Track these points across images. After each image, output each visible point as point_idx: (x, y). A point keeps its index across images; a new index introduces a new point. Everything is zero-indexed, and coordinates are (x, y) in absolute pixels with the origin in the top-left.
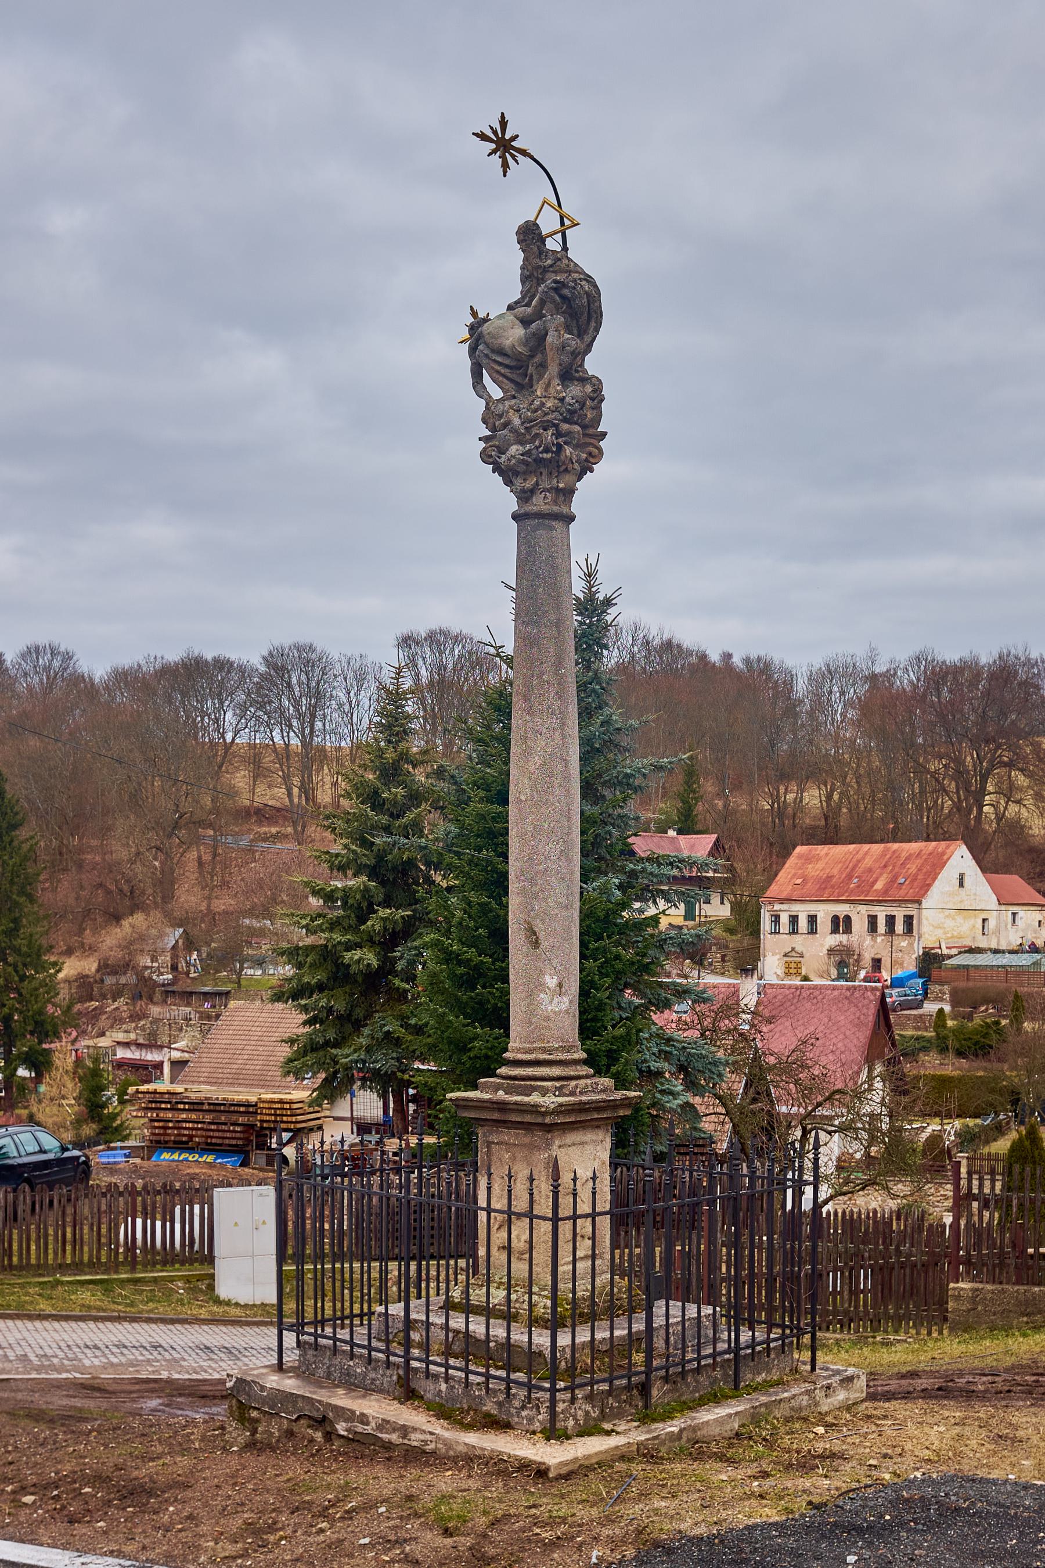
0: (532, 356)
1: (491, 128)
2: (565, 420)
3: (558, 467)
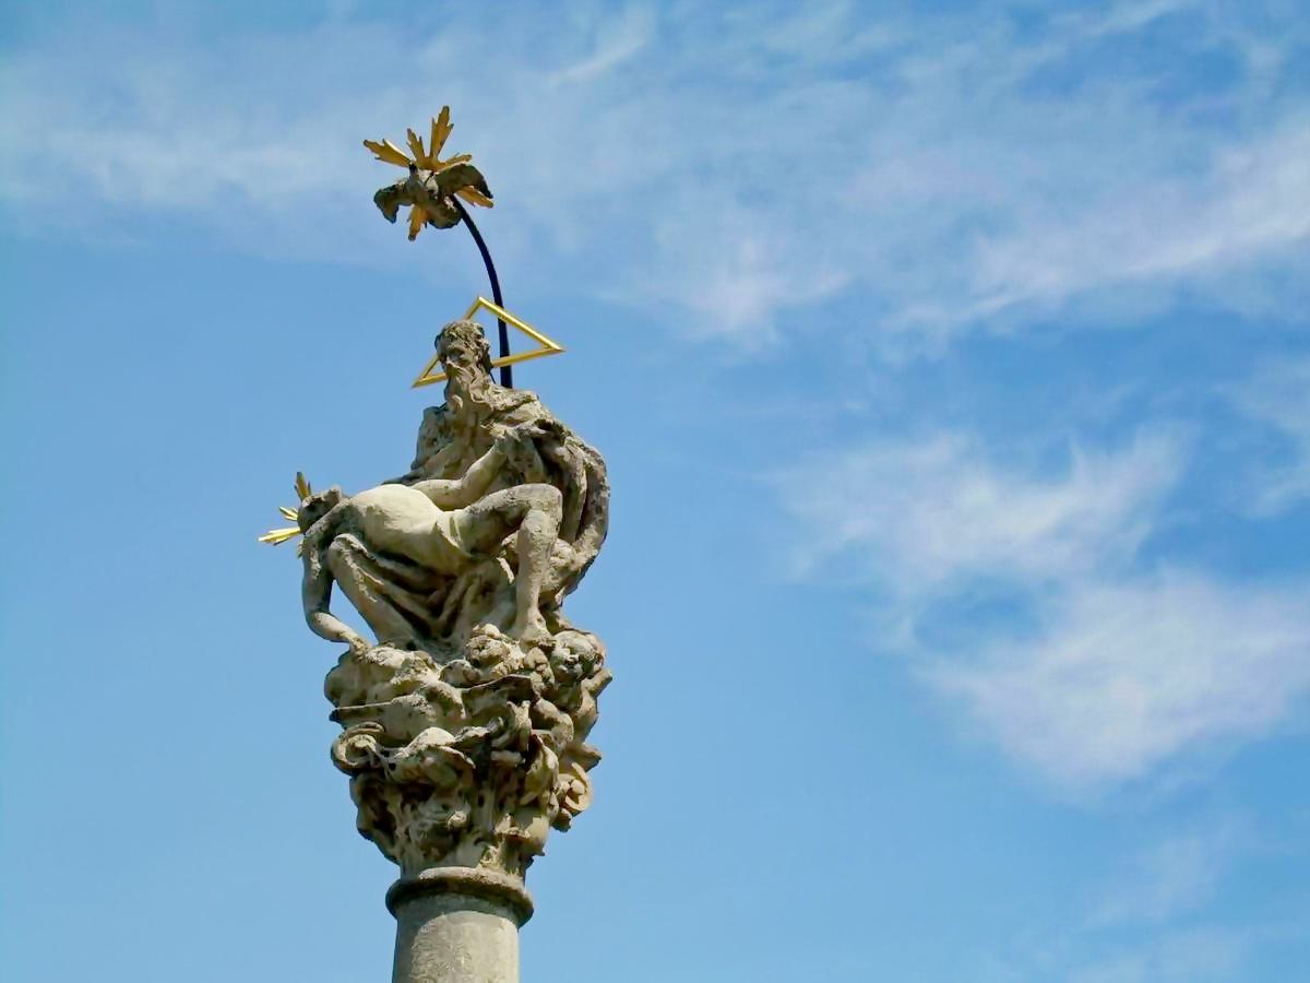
0: (473, 563)
1: (411, 135)
2: (549, 695)
3: (520, 793)
